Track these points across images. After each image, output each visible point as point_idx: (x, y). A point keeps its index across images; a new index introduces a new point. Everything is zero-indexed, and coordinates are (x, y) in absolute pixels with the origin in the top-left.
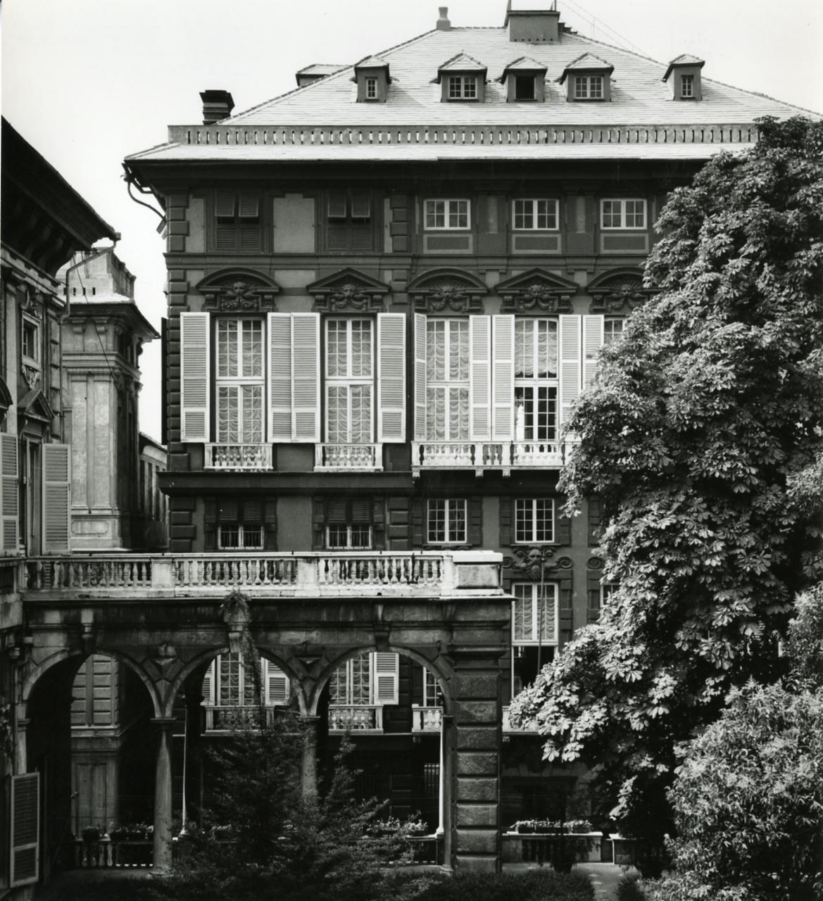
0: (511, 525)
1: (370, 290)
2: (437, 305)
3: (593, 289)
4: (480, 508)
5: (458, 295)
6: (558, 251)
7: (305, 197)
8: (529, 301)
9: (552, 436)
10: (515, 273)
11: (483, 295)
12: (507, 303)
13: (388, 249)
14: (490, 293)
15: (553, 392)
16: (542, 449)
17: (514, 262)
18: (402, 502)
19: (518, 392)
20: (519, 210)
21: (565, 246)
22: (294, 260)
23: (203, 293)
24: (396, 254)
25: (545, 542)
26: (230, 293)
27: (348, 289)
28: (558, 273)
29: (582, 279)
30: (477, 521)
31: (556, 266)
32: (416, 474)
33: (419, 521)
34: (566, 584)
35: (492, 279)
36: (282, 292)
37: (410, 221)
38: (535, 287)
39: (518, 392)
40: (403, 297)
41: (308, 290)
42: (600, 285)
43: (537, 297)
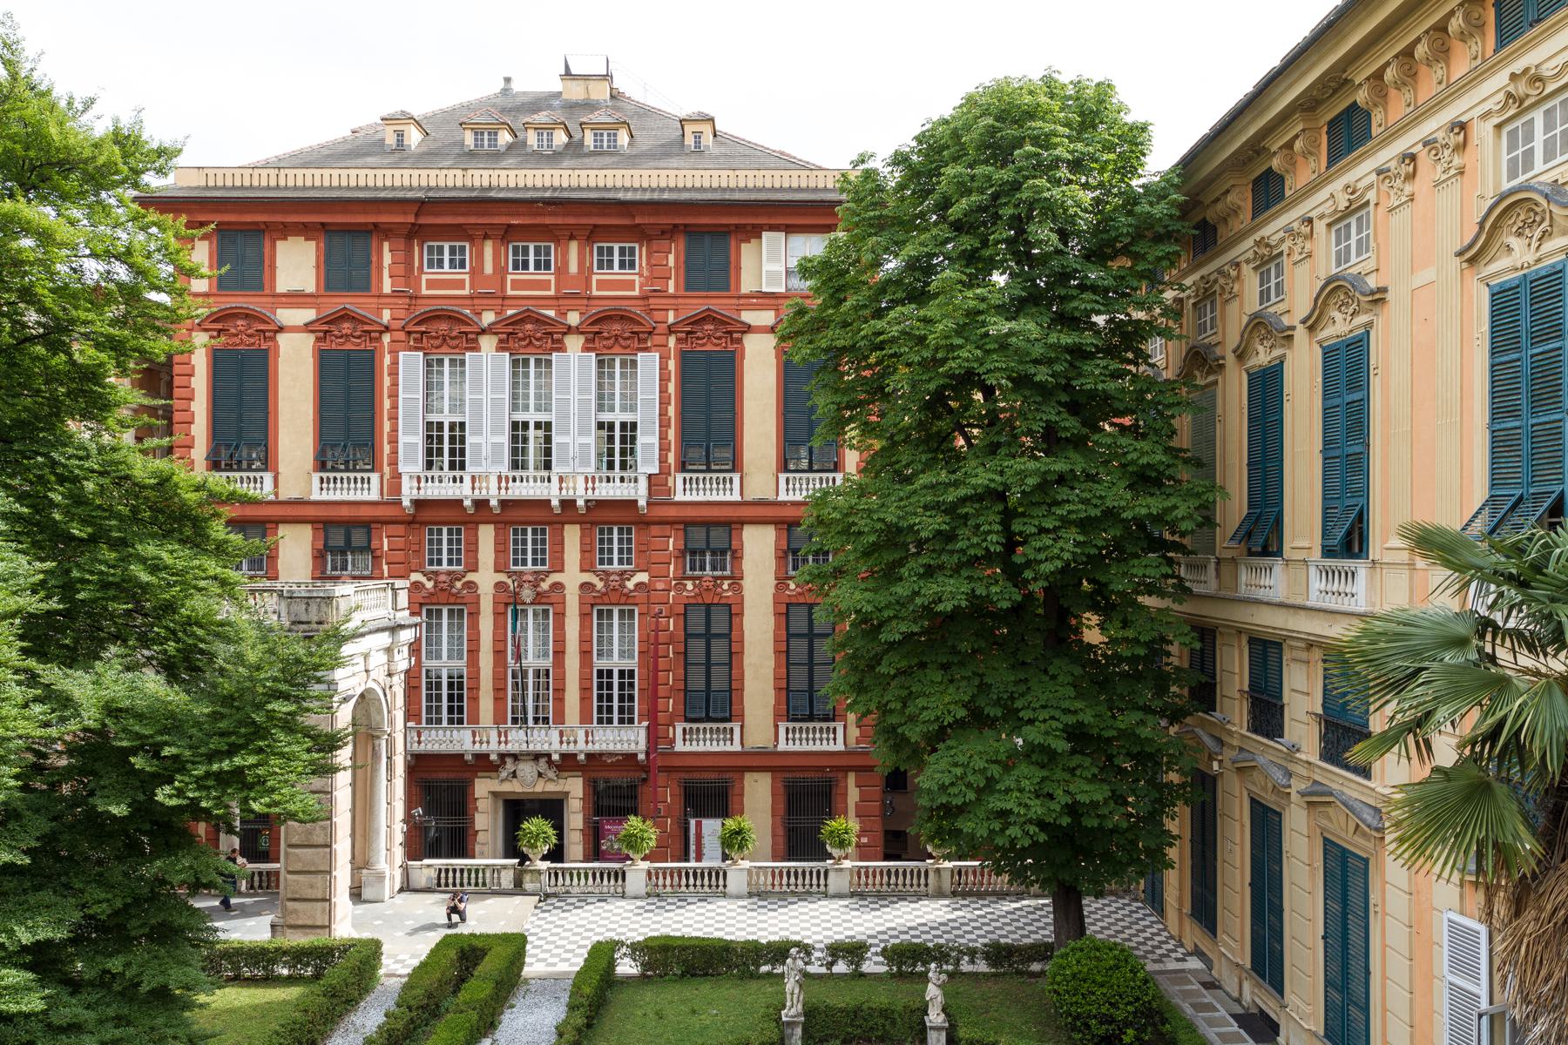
0: (506, 551)
1: (366, 328)
2: (437, 342)
3: (584, 328)
4: (476, 535)
5: (454, 334)
6: (552, 293)
7: (307, 239)
8: (523, 339)
9: (462, 467)
10: (510, 312)
11: (478, 334)
12: (501, 341)
13: (387, 287)
14: (483, 332)
15: (634, 426)
16: (622, 480)
17: (507, 302)
18: (400, 529)
19: (600, 426)
20: (516, 253)
21: (557, 289)
22: (296, 299)
23: (206, 330)
24: (396, 294)
25: (539, 568)
26: (233, 331)
27: (346, 327)
28: (551, 313)
29: (573, 318)
30: (472, 547)
31: (548, 307)
32: (406, 503)
33: (416, 547)
34: (559, 608)
35: (488, 318)
36: (281, 329)
37: (409, 263)
38: (529, 327)
39: (600, 426)
40: (401, 336)
41: (308, 328)
42: (592, 324)
43: (530, 337)
